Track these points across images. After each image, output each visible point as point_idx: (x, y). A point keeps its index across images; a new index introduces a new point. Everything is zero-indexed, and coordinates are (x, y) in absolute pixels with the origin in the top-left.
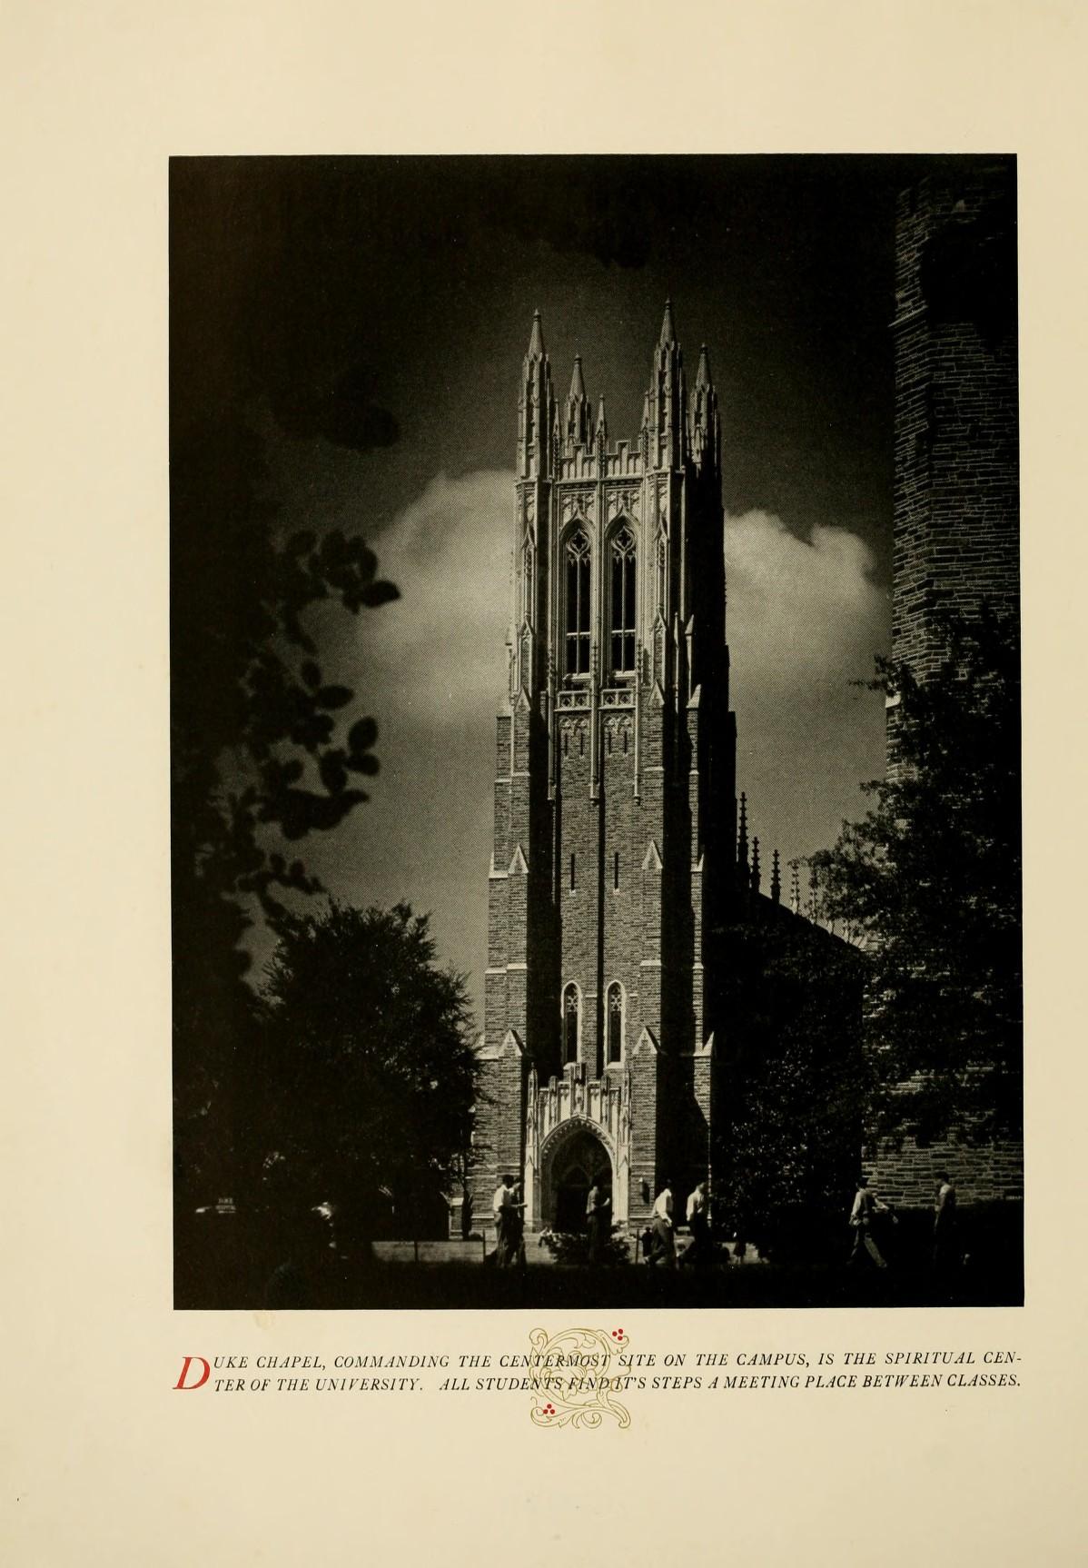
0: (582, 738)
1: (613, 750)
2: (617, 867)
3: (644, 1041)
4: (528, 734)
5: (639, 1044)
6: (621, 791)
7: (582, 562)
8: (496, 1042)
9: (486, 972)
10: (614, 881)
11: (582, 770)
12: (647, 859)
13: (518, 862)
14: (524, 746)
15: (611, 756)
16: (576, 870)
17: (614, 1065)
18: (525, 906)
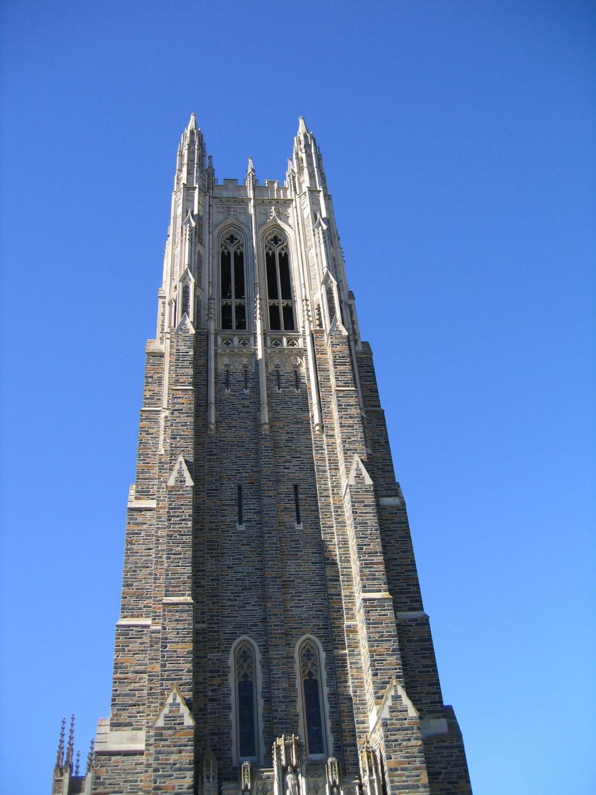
0: (246, 374)
1: (282, 385)
2: (297, 500)
3: (397, 698)
4: (191, 353)
5: (389, 703)
6: (297, 423)
7: (236, 253)
8: (132, 725)
9: (118, 623)
10: (295, 514)
11: (247, 403)
13: (180, 472)
14: (186, 363)
16: (244, 502)
18: (190, 524)
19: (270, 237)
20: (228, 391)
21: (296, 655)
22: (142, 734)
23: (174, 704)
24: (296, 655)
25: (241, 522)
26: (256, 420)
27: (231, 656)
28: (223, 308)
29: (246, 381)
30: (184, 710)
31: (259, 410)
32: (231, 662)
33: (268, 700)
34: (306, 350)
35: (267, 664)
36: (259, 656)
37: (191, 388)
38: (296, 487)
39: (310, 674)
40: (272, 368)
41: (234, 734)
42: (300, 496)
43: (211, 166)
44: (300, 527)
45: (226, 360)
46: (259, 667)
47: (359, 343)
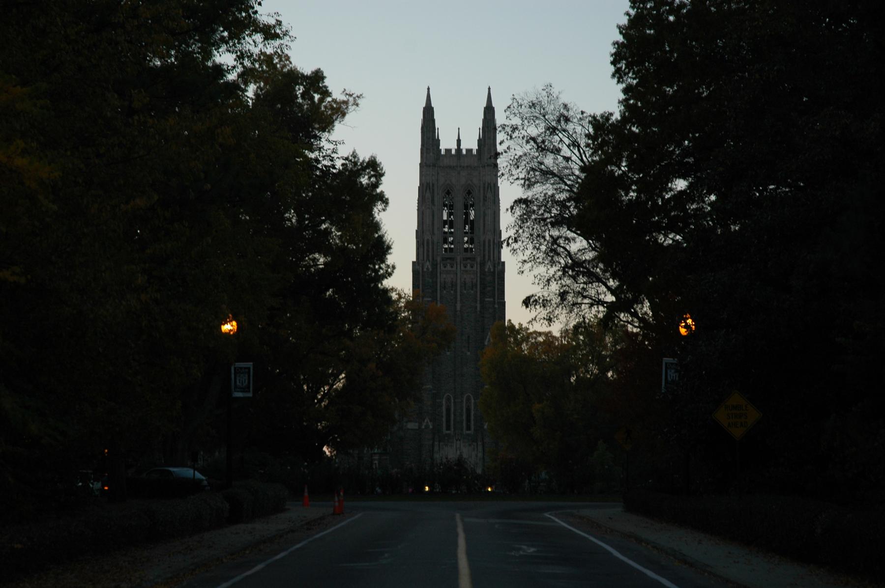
12: (487, 340)
15: (465, 292)
17: (468, 432)
19: (466, 192)
20: (445, 292)
21: (464, 401)
22: (417, 424)
23: (427, 422)
24: (464, 401)
25: (448, 351)
26: (455, 307)
27: (444, 400)
28: (444, 238)
29: (452, 285)
30: (430, 423)
31: (456, 303)
32: (444, 403)
33: (455, 415)
34: (477, 272)
35: (455, 402)
36: (452, 401)
37: (430, 299)
38: (469, 337)
39: (468, 406)
40: (463, 280)
41: (444, 425)
42: (470, 341)
43: (438, 141)
44: (469, 353)
45: (444, 276)
46: (452, 404)
47: (501, 264)
